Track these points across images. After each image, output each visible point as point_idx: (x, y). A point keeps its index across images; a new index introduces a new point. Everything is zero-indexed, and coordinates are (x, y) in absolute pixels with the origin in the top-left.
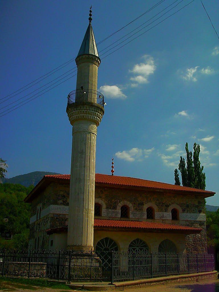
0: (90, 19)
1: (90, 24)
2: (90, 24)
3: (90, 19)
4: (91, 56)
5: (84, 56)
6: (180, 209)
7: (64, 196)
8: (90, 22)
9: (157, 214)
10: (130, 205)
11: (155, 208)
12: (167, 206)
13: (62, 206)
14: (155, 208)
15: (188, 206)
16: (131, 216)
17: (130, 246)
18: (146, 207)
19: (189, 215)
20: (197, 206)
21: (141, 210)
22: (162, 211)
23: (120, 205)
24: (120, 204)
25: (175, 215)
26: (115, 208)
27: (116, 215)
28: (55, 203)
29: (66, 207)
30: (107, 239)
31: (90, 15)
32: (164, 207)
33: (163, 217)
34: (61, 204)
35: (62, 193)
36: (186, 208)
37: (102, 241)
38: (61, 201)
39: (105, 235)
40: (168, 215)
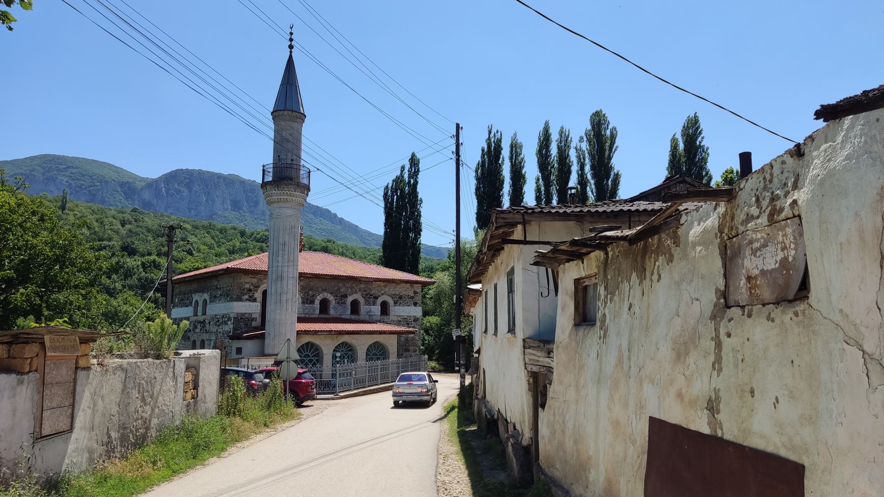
0: (291, 47)
1: (291, 56)
2: (291, 56)
3: (291, 47)
4: (294, 114)
5: (286, 113)
6: (391, 301)
7: (250, 290)
8: (291, 52)
9: (363, 308)
10: (331, 298)
11: (362, 300)
12: (376, 298)
13: (248, 303)
14: (362, 300)
15: (401, 297)
16: (332, 312)
17: (334, 350)
18: (350, 299)
19: (401, 308)
20: (412, 298)
21: (344, 303)
22: (369, 304)
23: (319, 298)
24: (318, 298)
25: (385, 309)
26: (312, 302)
27: (314, 310)
28: (239, 299)
29: (253, 304)
30: (308, 343)
31: (291, 40)
32: (371, 298)
33: (370, 311)
34: (247, 300)
35: (247, 286)
36: (399, 300)
37: (302, 346)
38: (246, 297)
39: (306, 339)
40: (376, 309)
